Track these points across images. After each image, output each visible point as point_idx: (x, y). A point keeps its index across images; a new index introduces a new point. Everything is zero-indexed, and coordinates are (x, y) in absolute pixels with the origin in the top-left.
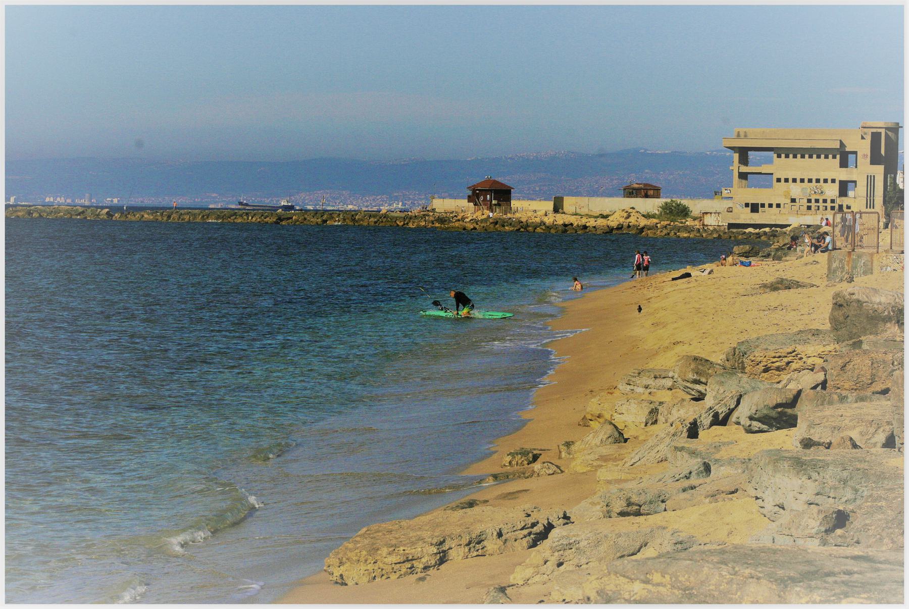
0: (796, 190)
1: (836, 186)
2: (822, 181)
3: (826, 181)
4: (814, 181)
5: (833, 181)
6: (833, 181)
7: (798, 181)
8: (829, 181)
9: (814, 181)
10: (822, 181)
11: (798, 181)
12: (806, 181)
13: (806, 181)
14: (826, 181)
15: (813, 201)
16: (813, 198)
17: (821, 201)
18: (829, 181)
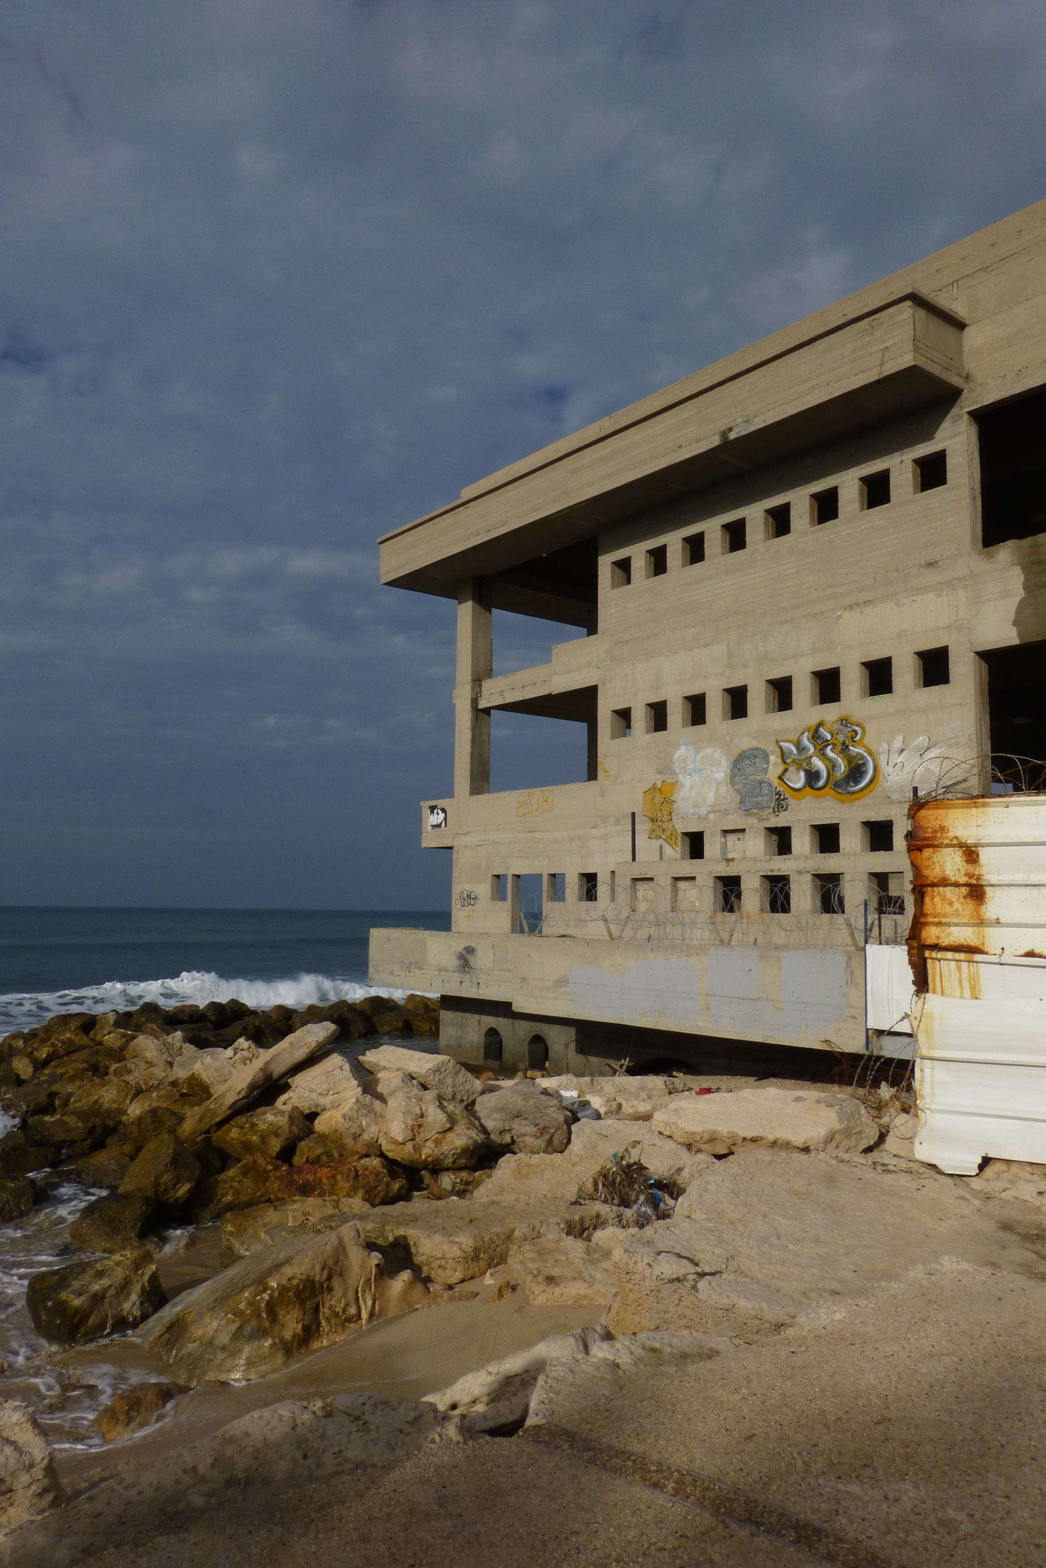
0: (701, 773)
1: (963, 696)
2: (853, 682)
3: (879, 677)
4: (803, 691)
5: (934, 667)
6: (934, 667)
7: (716, 706)
8: (905, 673)
9: (803, 691)
10: (853, 682)
11: (716, 706)
12: (757, 699)
13: (757, 699)
14: (879, 677)
15: (802, 842)
16: (803, 815)
17: (852, 839)
18: (905, 673)
